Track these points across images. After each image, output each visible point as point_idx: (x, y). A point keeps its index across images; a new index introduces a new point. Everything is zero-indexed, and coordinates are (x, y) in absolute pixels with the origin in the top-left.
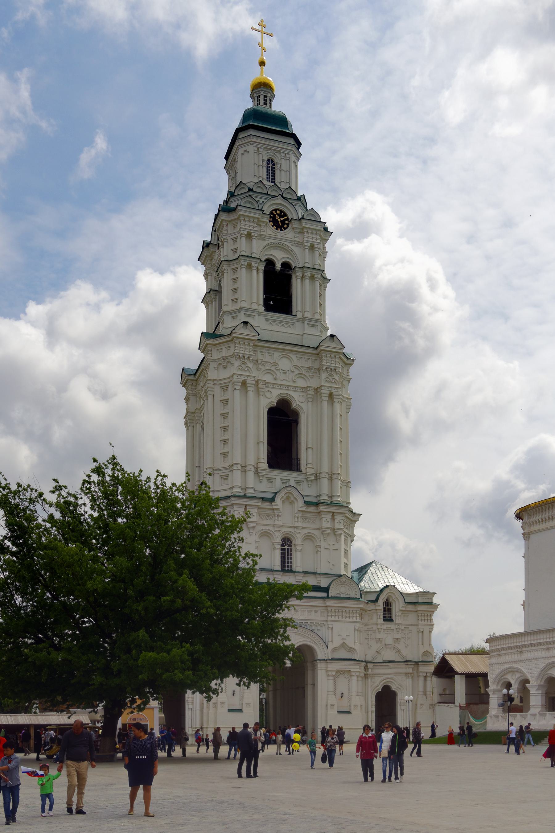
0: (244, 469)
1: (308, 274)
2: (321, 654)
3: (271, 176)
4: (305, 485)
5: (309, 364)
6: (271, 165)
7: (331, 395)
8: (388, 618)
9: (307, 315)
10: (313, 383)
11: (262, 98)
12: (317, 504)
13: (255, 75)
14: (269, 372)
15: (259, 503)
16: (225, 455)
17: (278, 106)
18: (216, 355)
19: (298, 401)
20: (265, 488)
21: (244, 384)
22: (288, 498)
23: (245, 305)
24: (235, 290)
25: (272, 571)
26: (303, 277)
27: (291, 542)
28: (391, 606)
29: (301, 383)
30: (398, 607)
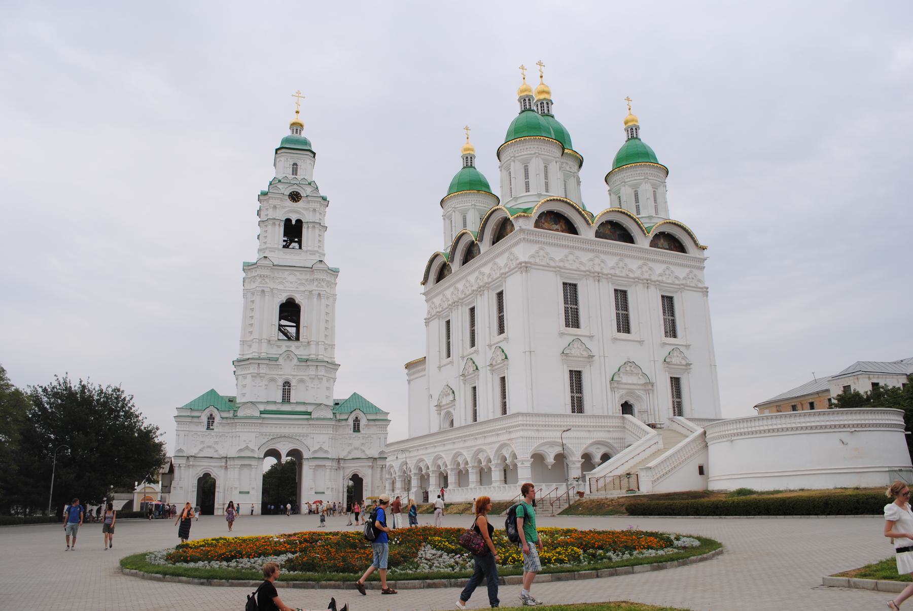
0: (260, 341)
1: (310, 225)
2: (305, 456)
4: (302, 349)
5: (308, 277)
7: (319, 294)
8: (357, 428)
9: (309, 248)
10: (309, 288)
12: (307, 360)
13: (294, 118)
14: (281, 283)
15: (267, 362)
16: (251, 332)
17: (305, 134)
18: (250, 275)
19: (299, 299)
20: (274, 352)
21: (263, 291)
23: (268, 245)
24: (266, 237)
25: (275, 403)
29: (302, 288)
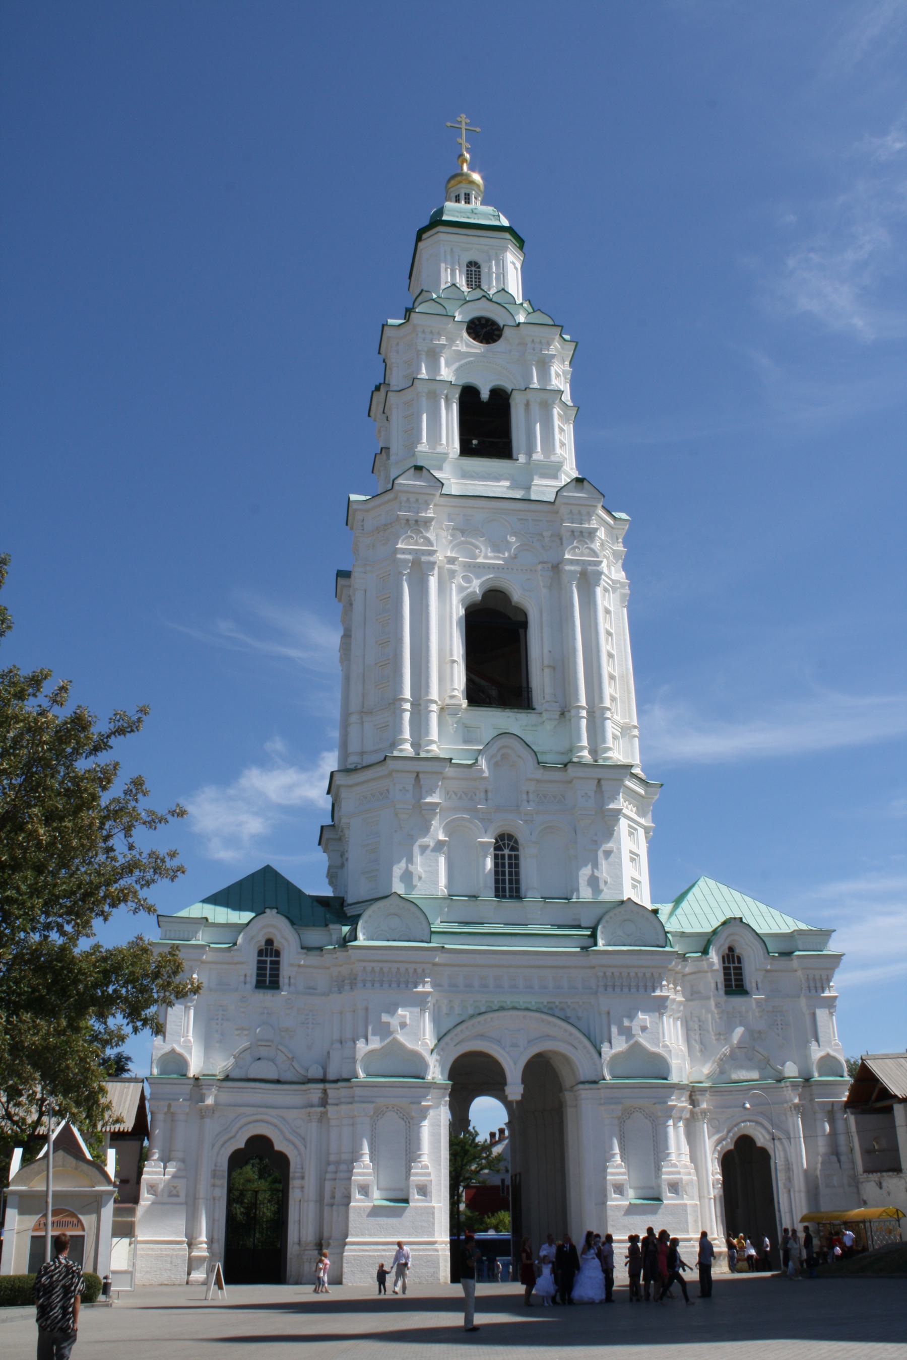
6: (473, 269)
22: (504, 757)
26: (527, 405)
27: (516, 842)
28: (739, 961)
30: (754, 967)
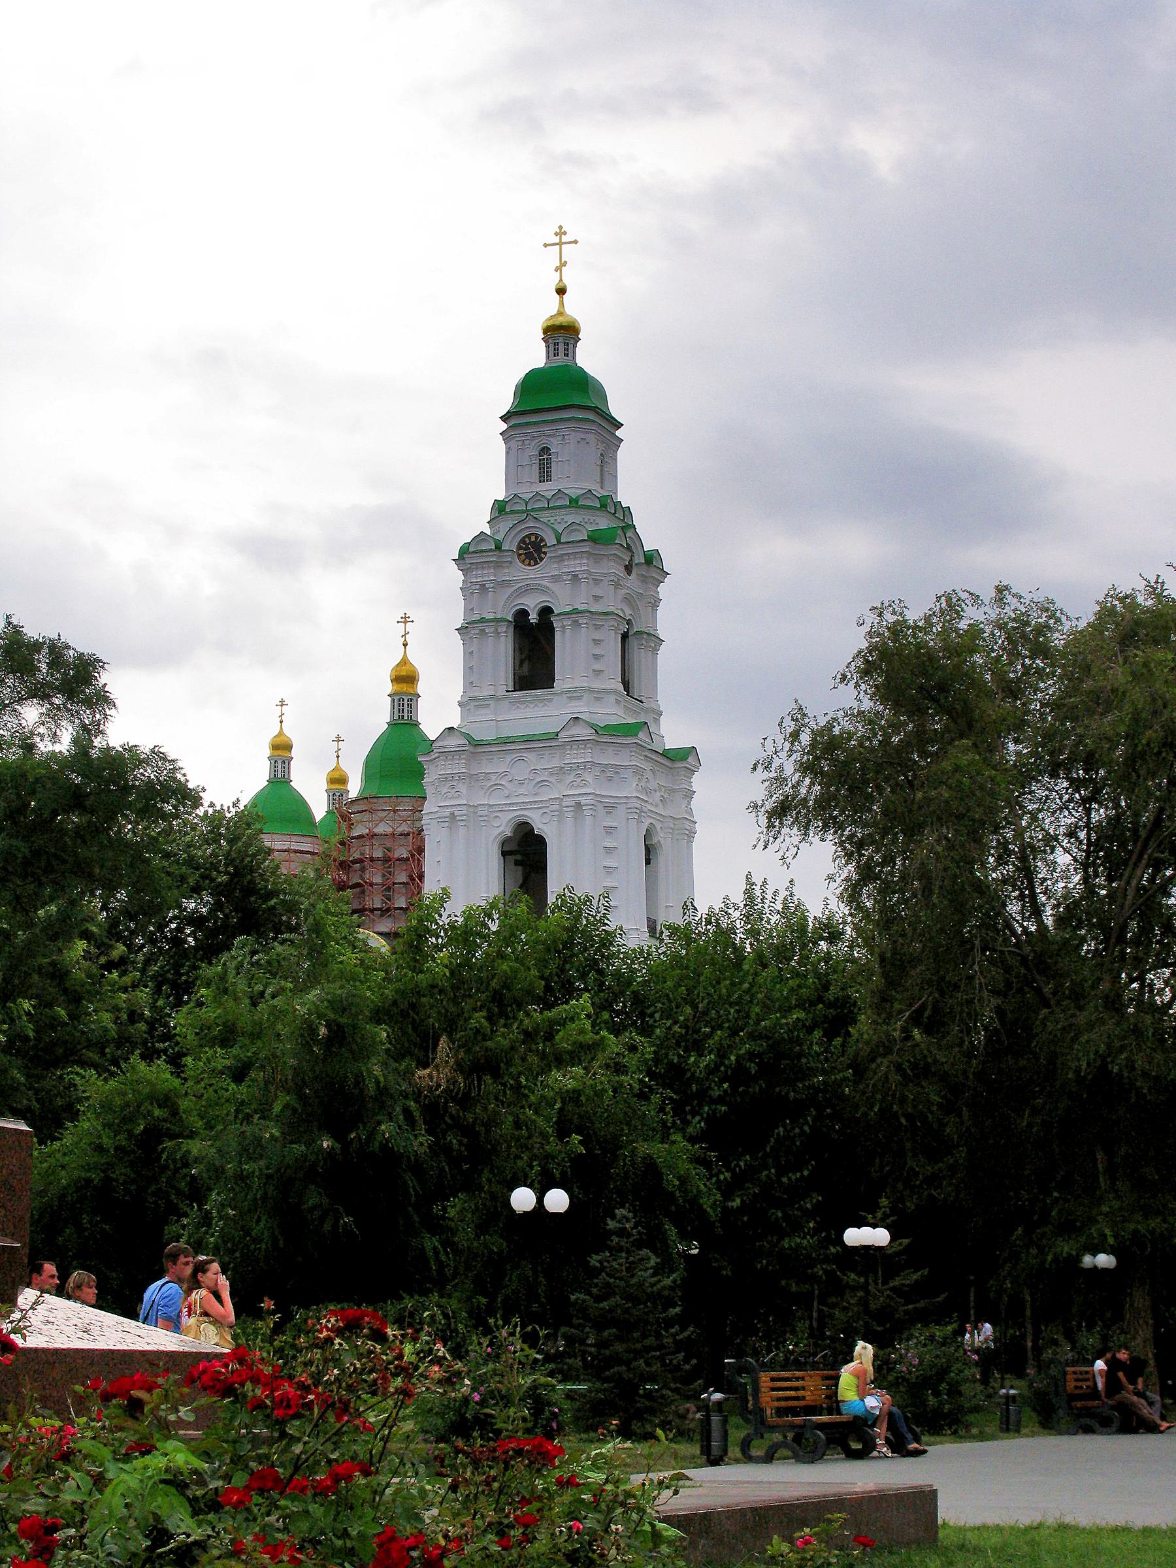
3: (545, 474)
7: (578, 804)
11: (561, 347)
14: (497, 787)
26: (563, 627)
